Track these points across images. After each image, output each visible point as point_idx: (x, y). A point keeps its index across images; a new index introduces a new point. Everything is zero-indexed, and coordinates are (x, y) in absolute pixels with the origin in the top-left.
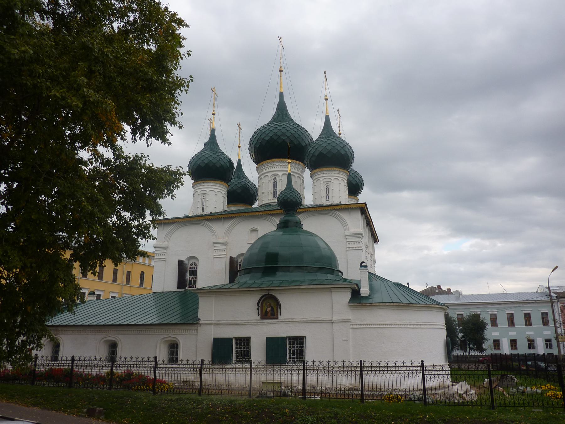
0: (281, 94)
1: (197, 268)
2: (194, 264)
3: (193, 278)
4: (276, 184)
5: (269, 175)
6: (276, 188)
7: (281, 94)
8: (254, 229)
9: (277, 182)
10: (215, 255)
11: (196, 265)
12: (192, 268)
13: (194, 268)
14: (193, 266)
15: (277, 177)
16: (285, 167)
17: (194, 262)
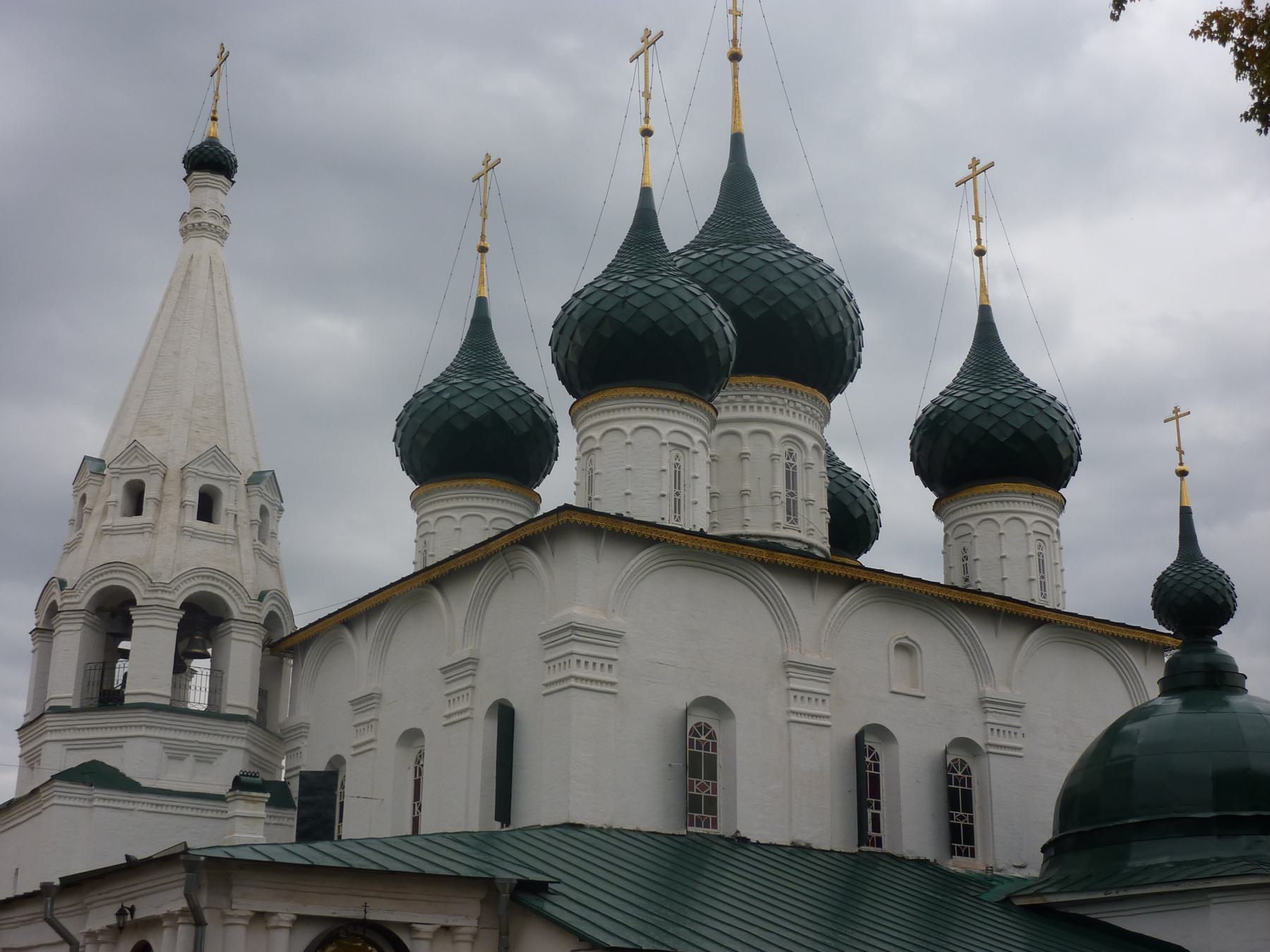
0: (737, 142)
1: (714, 745)
2: (700, 729)
3: (703, 787)
4: (795, 474)
5: (778, 433)
6: (795, 487)
7: (737, 142)
8: (905, 641)
9: (795, 468)
10: (793, 712)
11: (709, 737)
12: (699, 747)
13: (707, 748)
14: (703, 738)
15: (796, 451)
16: (744, 407)
17: (703, 721)
